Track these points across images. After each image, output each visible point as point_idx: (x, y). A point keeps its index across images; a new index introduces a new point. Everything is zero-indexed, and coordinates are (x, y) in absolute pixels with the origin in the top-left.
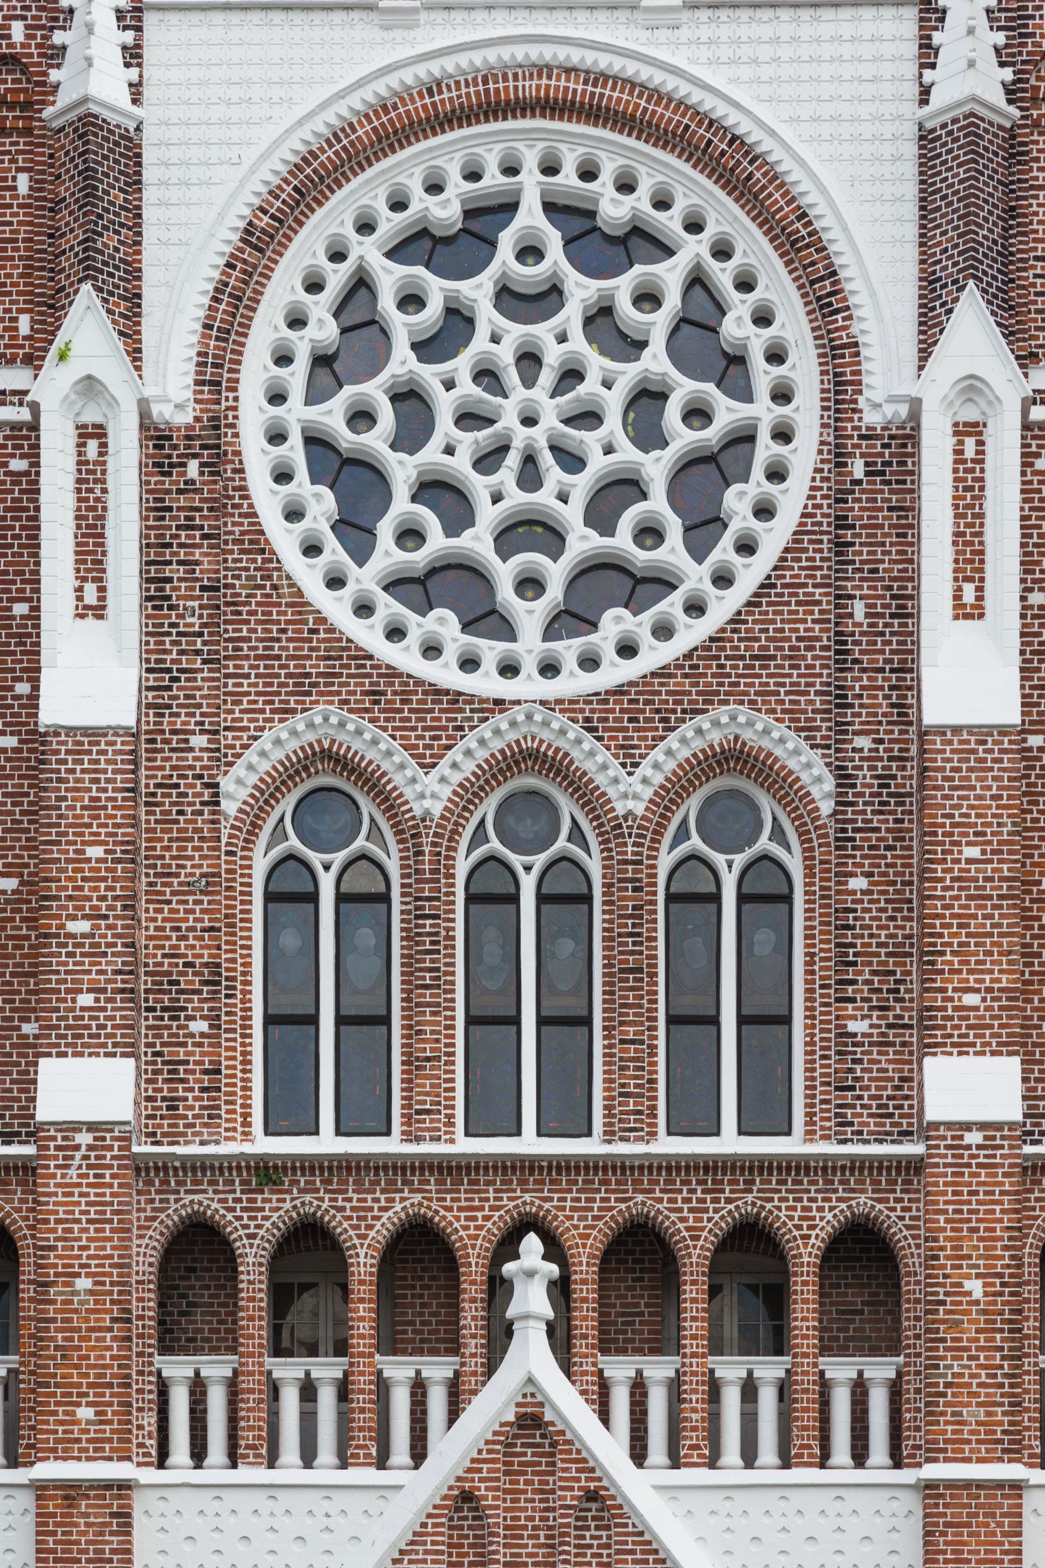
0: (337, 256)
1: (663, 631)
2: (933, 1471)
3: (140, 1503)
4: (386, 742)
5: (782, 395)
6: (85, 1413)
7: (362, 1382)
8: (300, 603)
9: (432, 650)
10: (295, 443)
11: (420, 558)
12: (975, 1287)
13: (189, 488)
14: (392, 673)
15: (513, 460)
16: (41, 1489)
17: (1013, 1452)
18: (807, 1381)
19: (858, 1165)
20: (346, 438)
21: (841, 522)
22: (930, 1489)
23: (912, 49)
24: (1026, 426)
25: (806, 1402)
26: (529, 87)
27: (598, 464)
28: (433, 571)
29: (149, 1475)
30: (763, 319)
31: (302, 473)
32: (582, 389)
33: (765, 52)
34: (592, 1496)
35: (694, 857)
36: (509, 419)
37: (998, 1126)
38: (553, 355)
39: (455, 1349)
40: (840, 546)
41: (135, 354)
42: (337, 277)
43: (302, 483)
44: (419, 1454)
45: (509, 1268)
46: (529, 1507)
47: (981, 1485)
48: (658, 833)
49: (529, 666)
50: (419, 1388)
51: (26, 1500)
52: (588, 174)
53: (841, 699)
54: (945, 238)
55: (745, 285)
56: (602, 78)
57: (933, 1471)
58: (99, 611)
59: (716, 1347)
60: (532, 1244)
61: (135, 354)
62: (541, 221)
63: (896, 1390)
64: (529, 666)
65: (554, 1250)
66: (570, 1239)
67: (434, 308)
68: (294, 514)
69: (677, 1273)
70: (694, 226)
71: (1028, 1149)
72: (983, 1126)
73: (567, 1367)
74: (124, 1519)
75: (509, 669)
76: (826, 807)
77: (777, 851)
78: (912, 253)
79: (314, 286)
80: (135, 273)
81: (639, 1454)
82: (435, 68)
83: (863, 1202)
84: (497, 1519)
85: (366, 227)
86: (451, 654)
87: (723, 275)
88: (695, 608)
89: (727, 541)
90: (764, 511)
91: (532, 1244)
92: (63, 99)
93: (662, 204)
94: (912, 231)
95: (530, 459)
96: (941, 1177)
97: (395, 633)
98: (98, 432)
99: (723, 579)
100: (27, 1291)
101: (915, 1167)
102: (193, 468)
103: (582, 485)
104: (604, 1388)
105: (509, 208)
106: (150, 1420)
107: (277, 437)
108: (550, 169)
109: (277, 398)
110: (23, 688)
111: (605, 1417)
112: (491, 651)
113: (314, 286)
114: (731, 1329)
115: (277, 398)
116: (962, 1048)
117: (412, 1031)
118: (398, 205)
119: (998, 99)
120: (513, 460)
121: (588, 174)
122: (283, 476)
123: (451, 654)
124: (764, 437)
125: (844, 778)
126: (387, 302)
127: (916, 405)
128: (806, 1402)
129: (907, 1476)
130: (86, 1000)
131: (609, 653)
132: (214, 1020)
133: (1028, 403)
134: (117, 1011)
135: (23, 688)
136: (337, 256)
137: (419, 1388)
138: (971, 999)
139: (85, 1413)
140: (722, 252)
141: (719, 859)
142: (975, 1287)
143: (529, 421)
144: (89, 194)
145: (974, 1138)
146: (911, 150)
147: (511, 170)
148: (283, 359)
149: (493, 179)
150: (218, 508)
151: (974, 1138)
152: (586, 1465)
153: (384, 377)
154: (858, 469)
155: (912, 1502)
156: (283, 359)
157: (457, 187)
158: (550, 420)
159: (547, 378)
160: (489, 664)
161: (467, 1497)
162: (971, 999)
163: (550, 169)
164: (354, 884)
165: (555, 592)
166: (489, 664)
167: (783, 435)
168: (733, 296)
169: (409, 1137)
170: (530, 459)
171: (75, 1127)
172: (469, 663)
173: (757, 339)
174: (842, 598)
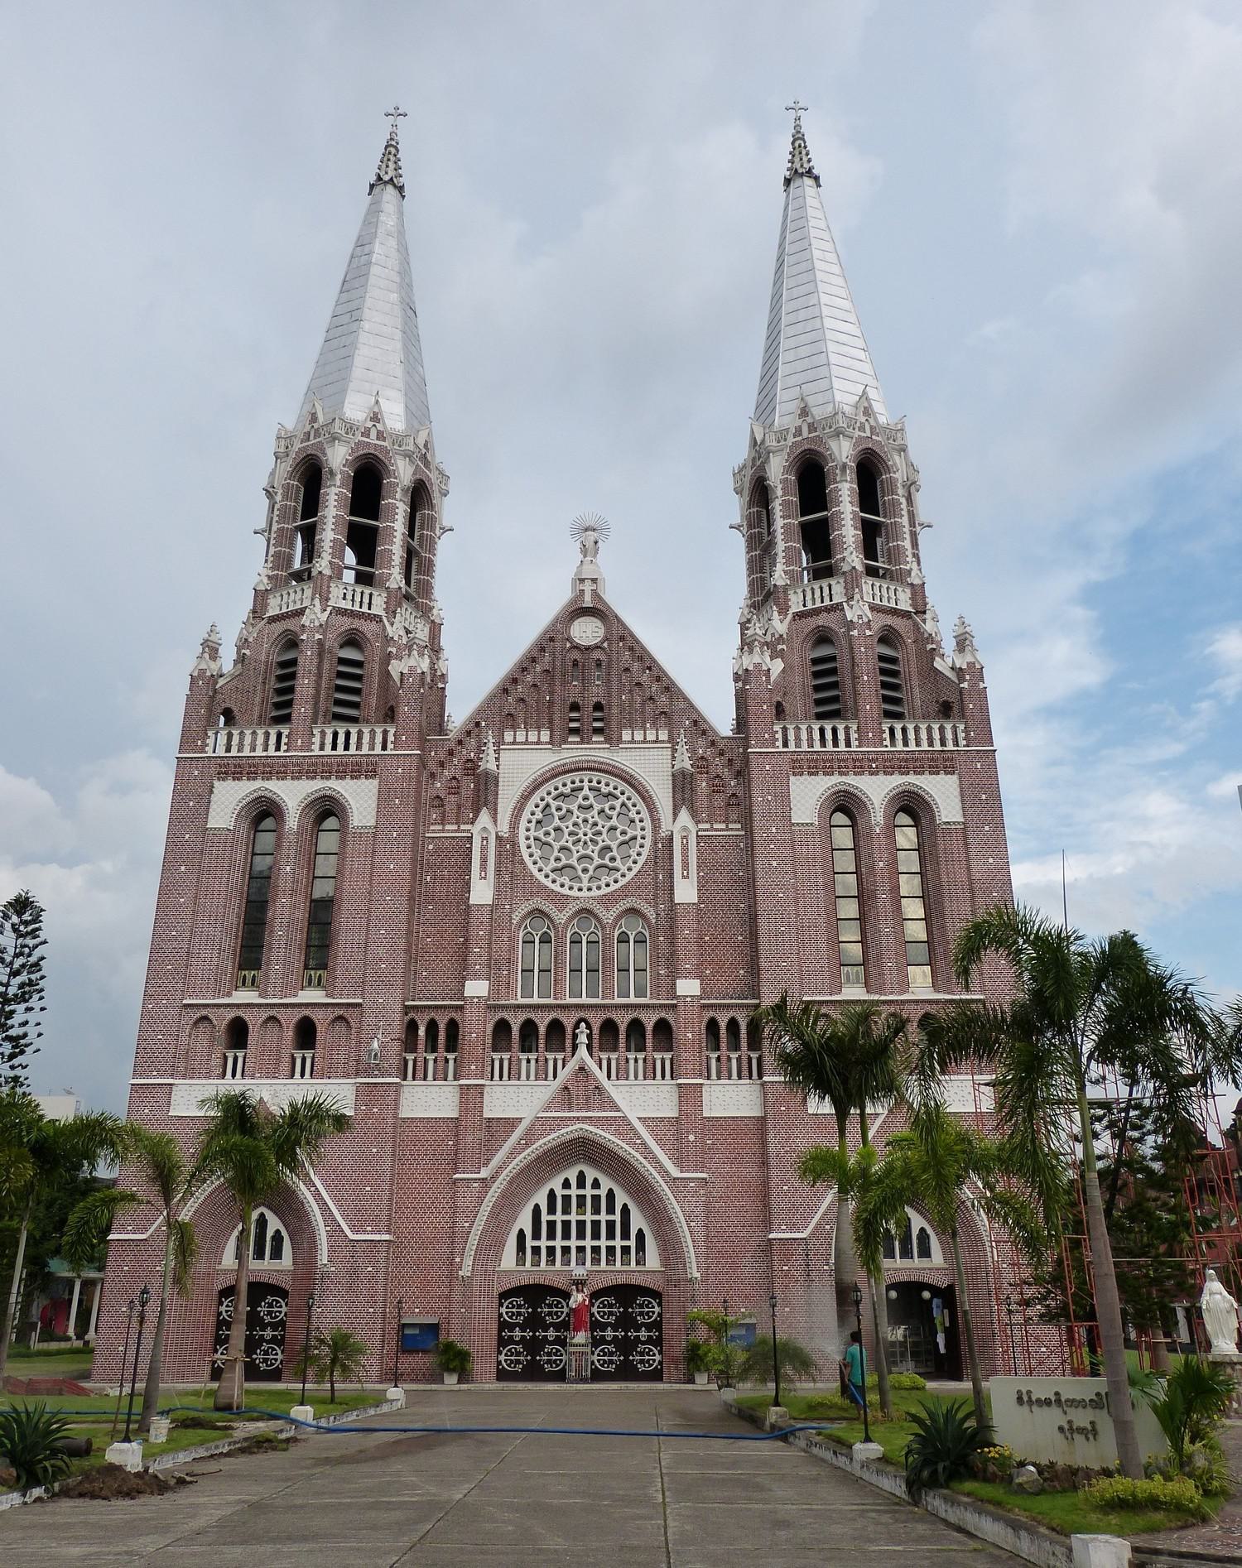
0: (542, 800)
1: (616, 881)
2: (680, 1081)
3: (486, 1089)
4: (551, 906)
5: (643, 829)
6: (473, 1067)
7: (541, 1059)
8: (532, 875)
9: (562, 886)
10: (532, 839)
11: (560, 865)
12: (690, 1035)
13: (507, 851)
14: (553, 891)
15: (581, 844)
16: (461, 1085)
17: (700, 1076)
18: (650, 1059)
19: (661, 1006)
20: (544, 839)
21: (656, 857)
22: (679, 1085)
23: (670, 757)
24: (697, 836)
25: (650, 1063)
26: (585, 765)
27: (601, 844)
28: (563, 868)
29: (488, 1083)
30: (638, 813)
31: (533, 847)
32: (598, 828)
33: (638, 758)
34: (597, 1088)
35: (623, 932)
36: (581, 835)
37: (481, 997)
38: (591, 821)
39: (564, 1051)
40: (656, 863)
41: (495, 822)
42: (542, 804)
43: (533, 849)
44: (555, 1077)
45: (577, 1031)
46: (582, 1089)
47: (693, 1084)
48: (615, 927)
49: (585, 889)
50: (555, 1061)
51: (458, 1089)
52: (599, 783)
53: (656, 896)
54: (679, 796)
55: (634, 806)
56: (602, 763)
57: (680, 1081)
58: (485, 878)
59: (628, 1050)
60: (583, 1025)
61: (495, 822)
62: (588, 792)
63: (672, 1060)
64: (585, 889)
65: (589, 1027)
66: (592, 1023)
67: (564, 810)
68: (531, 855)
69: (618, 1032)
70: (623, 793)
71: (702, 1002)
72: (478, 997)
73: (591, 1055)
74: (482, 1093)
75: (580, 889)
76: (654, 921)
77: (643, 931)
78: (671, 799)
79: (537, 806)
80: (496, 804)
81: (609, 1077)
82: (564, 761)
83: (663, 1015)
84: (574, 1093)
85: (549, 793)
86: (566, 887)
87: (629, 804)
88: (623, 875)
89: (631, 860)
90: (639, 854)
91: (583, 1025)
92: (481, 769)
93: (615, 788)
94: (671, 795)
95: (585, 843)
96: (681, 1009)
97: (554, 881)
98: (487, 839)
99: (630, 869)
100: (460, 1037)
101: (675, 1006)
102: (508, 846)
103: (597, 848)
104: (600, 1060)
105: (581, 789)
106: (489, 1069)
107: (528, 838)
108: (590, 781)
109: (528, 830)
110: (467, 895)
111: (601, 1068)
112: (576, 886)
113: (537, 806)
114: (633, 1046)
115: (528, 830)
116: (686, 978)
117: (556, 974)
118: (556, 789)
119: (690, 768)
120: (581, 844)
121: (599, 783)
122: (529, 847)
123: (566, 887)
124: (639, 838)
125: (658, 915)
126: (553, 810)
127: (672, 832)
128: (650, 1063)
129: (674, 1082)
130: (478, 967)
131: (603, 886)
132: (509, 970)
133: (697, 832)
134: (486, 970)
135: (467, 895)
136: (542, 800)
137: (555, 1061)
138: (687, 966)
139: (473, 1067)
140: (629, 799)
141: (629, 933)
142: (690, 1035)
143: (585, 835)
144: (487, 789)
145: (689, 999)
146: (671, 778)
147: (582, 781)
148: (530, 822)
149: (578, 784)
150: (514, 854)
151: (689, 999)
152: (596, 1080)
153: (552, 826)
154: (660, 846)
155: (675, 1089)
156: (530, 822)
157: (570, 785)
158: (590, 835)
159: (589, 826)
160: (576, 889)
161: (566, 1088)
162: (687, 966)
163: (590, 781)
164: (543, 939)
165: (591, 872)
166: (576, 889)
167: (643, 838)
168: (632, 808)
169: (556, 999)
170: (585, 843)
171: (474, 997)
172: (571, 888)
173: (637, 818)
174: (657, 874)
